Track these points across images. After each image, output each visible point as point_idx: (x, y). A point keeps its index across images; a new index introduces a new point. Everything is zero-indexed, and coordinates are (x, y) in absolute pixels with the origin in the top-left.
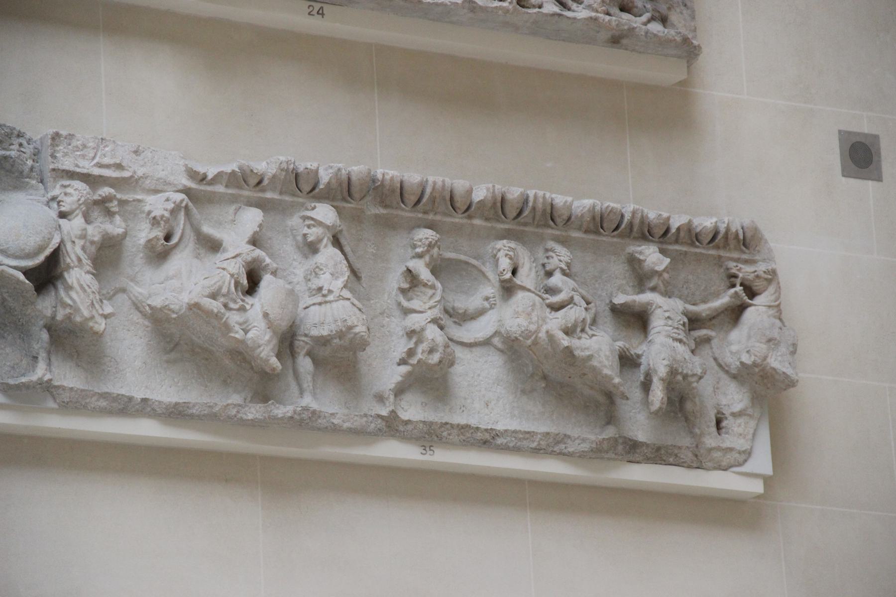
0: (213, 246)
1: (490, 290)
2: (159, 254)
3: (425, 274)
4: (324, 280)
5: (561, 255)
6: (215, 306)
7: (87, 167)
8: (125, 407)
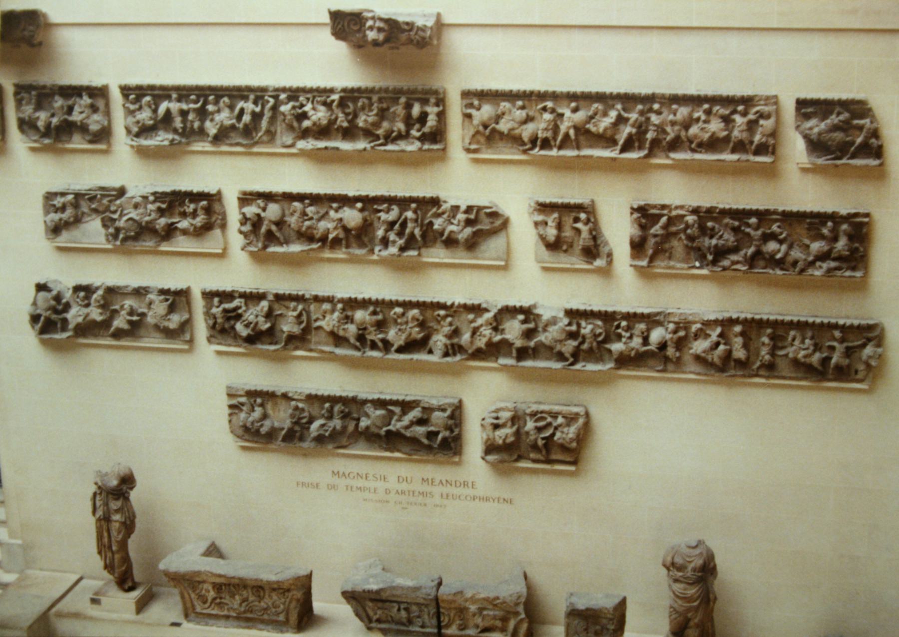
6: (703, 355)
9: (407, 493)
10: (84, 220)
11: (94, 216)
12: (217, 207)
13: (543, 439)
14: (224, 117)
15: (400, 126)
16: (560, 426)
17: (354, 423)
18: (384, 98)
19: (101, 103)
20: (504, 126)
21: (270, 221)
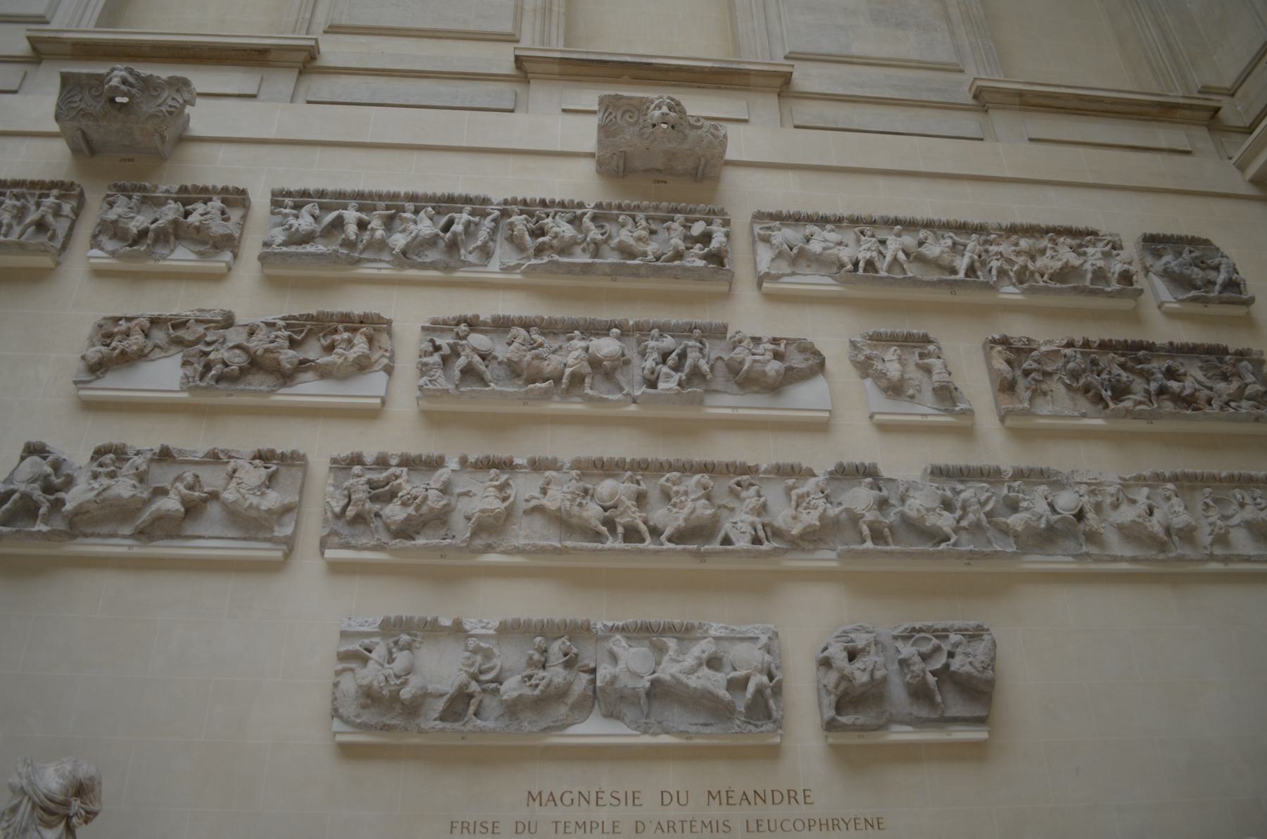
0: (1133, 502)
1: (1235, 507)
2: (1116, 506)
3: (1211, 503)
4: (1176, 508)
5: (1258, 492)
6: (1140, 520)
7: (1085, 480)
8: (1115, 559)
9: (678, 826)
10: (151, 356)
11: (174, 350)
12: (384, 339)
13: (934, 673)
14: (425, 226)
15: (677, 242)
16: (957, 645)
17: (585, 677)
18: (653, 218)
19: (235, 215)
20: (815, 247)
21: (474, 349)
